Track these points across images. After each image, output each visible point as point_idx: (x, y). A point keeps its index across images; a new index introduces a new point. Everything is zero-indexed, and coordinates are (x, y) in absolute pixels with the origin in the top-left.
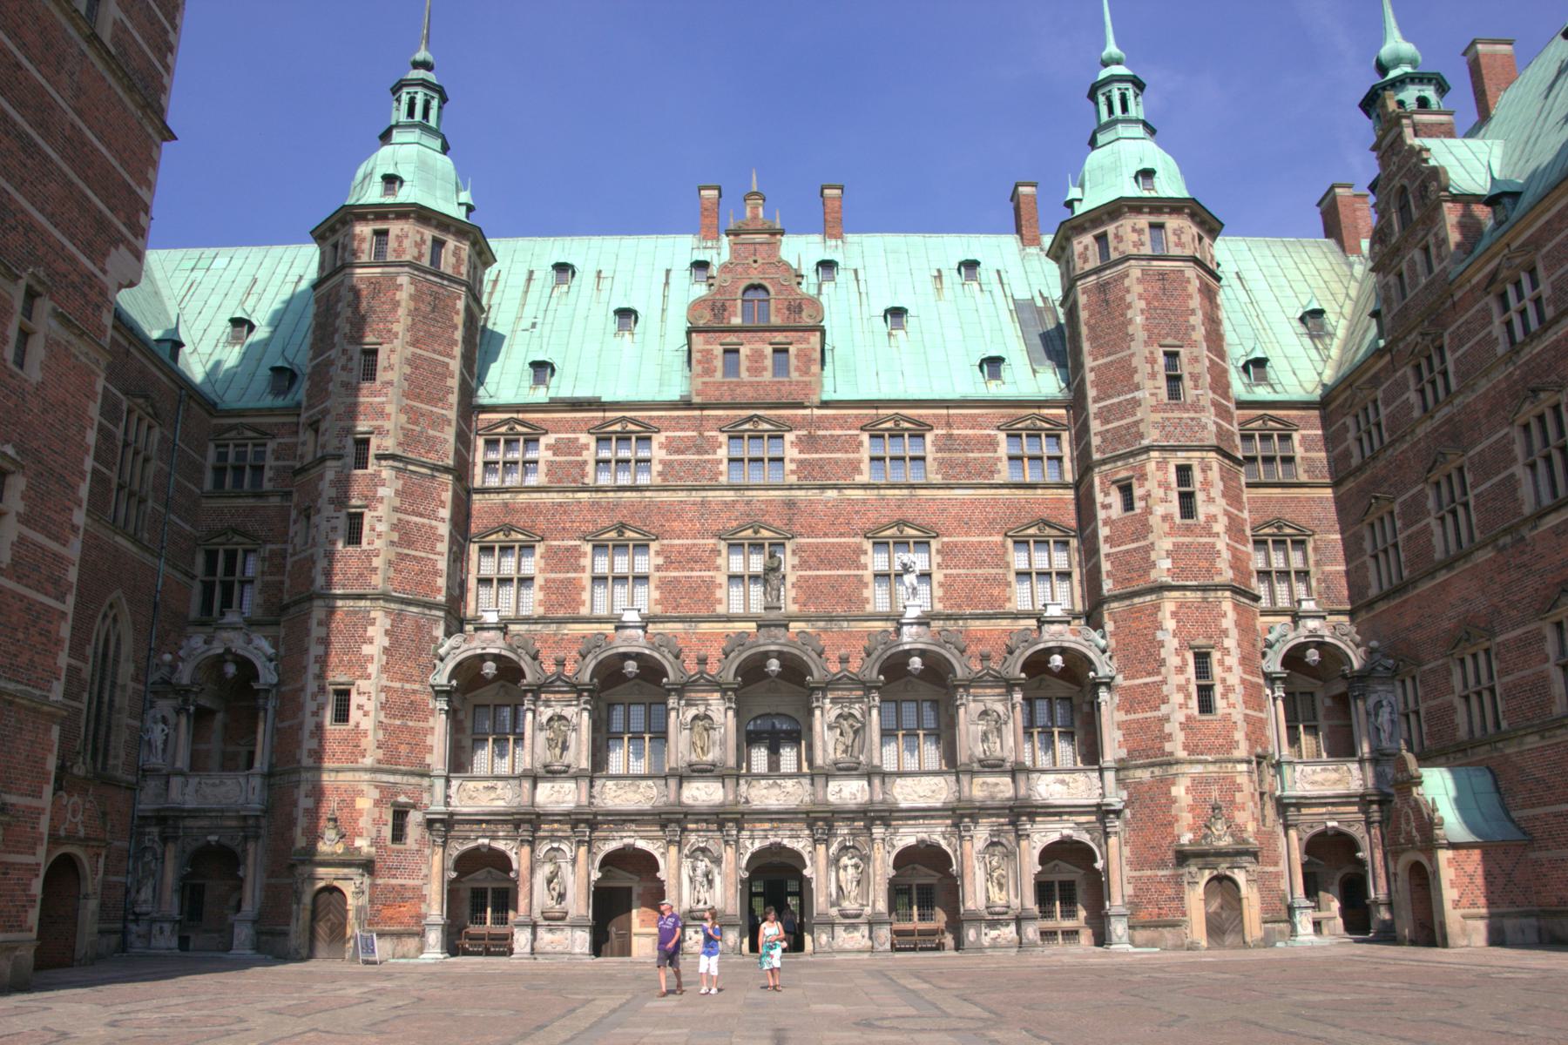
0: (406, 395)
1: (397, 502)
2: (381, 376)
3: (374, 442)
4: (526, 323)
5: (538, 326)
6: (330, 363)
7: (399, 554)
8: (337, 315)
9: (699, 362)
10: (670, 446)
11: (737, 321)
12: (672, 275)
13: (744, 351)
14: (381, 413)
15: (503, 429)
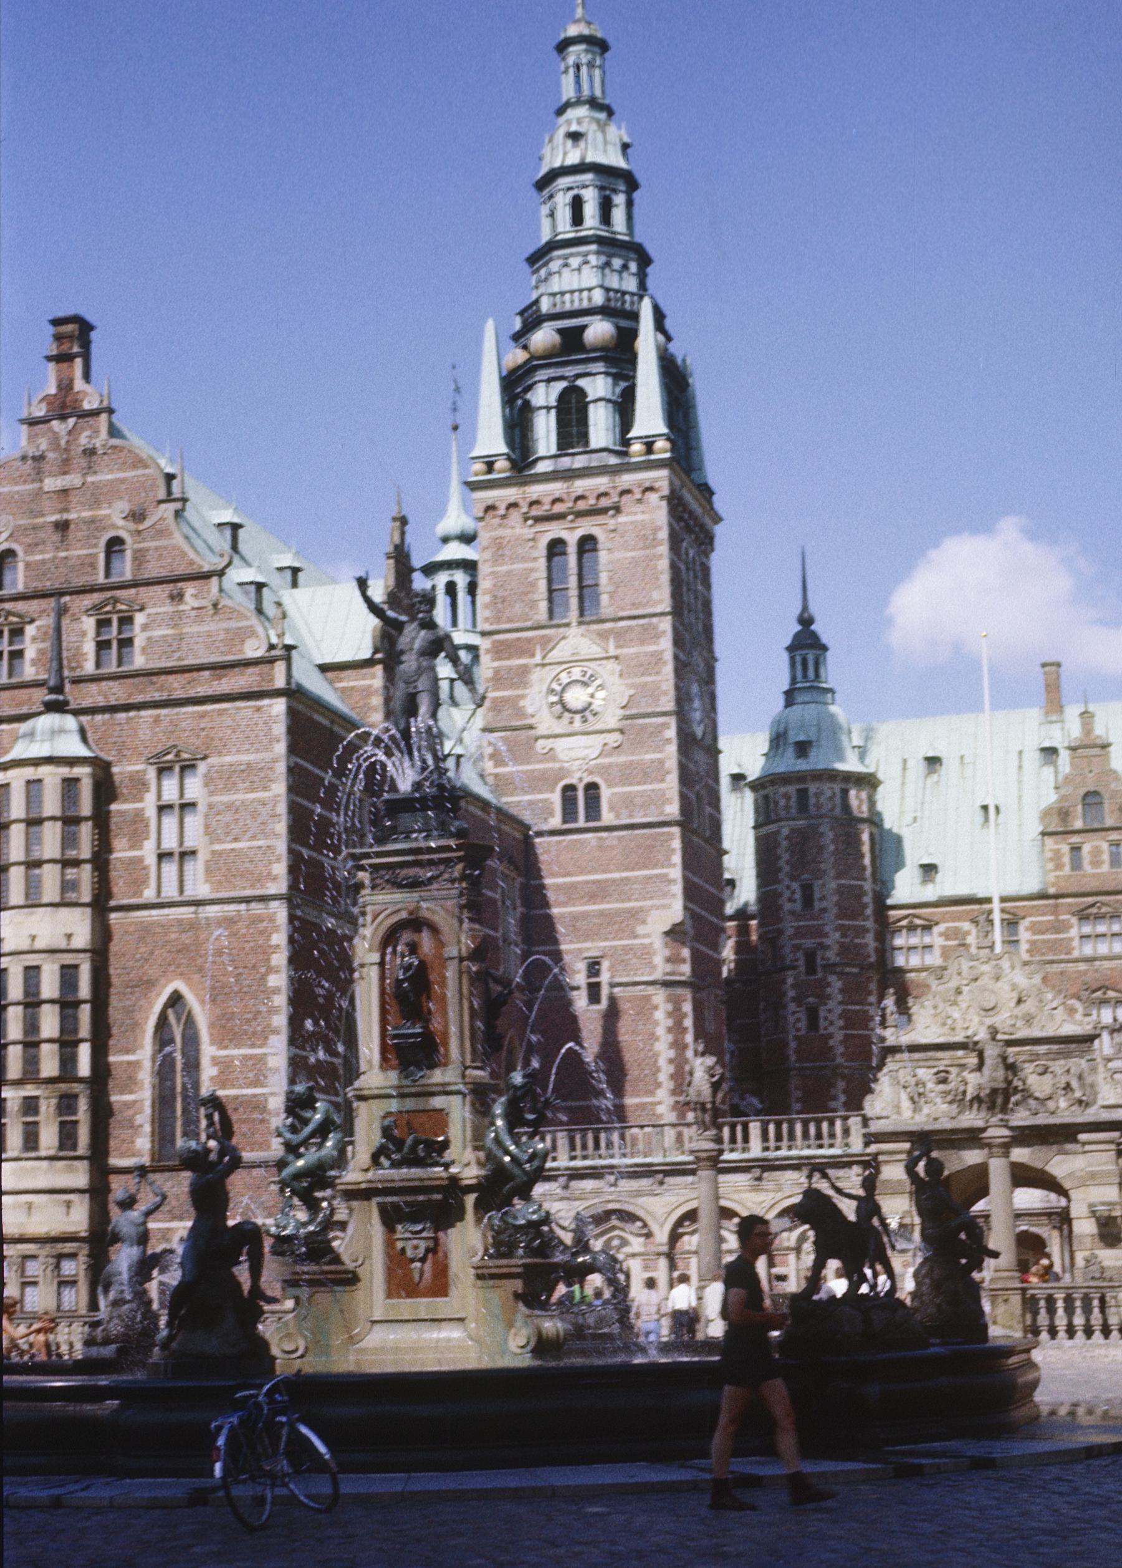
0: (838, 917)
1: (840, 997)
2: (817, 905)
3: (819, 954)
4: (908, 818)
5: (918, 820)
6: (778, 895)
7: (846, 1035)
8: (779, 858)
9: (1051, 859)
10: (1034, 928)
11: (1078, 824)
12: (1025, 756)
13: (1086, 849)
14: (820, 933)
15: (904, 923)
